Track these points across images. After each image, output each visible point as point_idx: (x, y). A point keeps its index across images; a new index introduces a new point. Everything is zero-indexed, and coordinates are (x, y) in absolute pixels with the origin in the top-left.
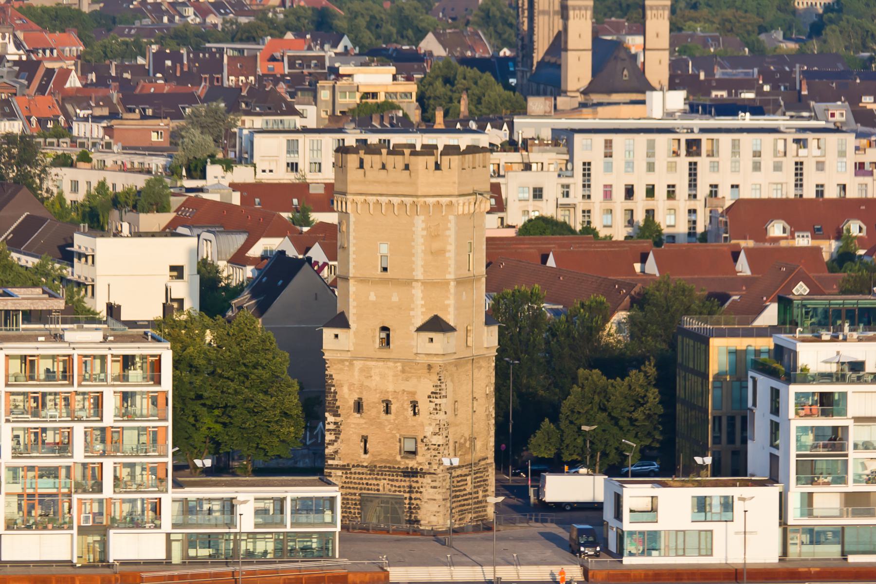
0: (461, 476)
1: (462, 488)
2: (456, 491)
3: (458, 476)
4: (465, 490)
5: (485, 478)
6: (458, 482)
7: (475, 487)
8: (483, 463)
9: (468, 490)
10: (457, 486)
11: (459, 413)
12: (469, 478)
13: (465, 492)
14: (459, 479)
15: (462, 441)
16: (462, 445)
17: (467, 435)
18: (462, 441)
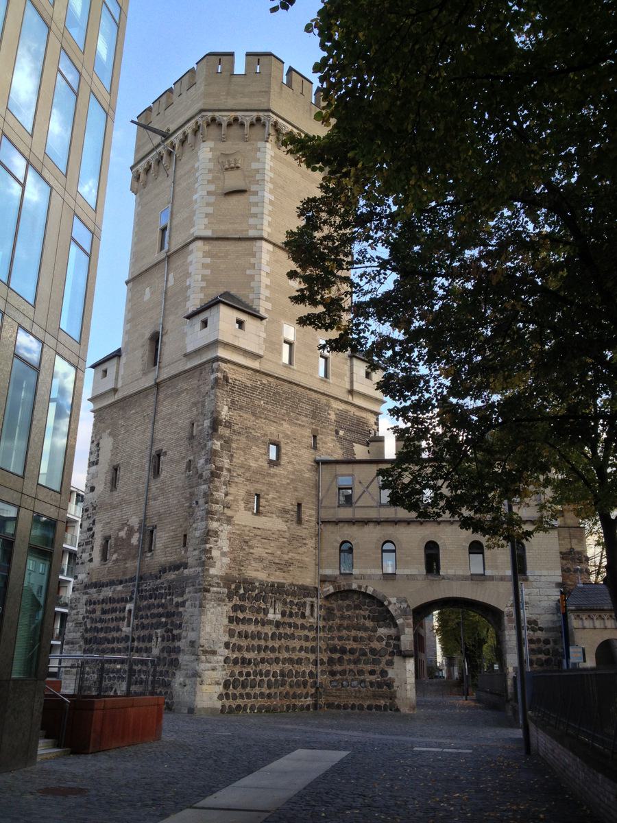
0: (112, 600)
1: (112, 625)
2: (98, 630)
3: (103, 601)
4: (118, 629)
5: (171, 609)
6: (104, 612)
7: (143, 627)
8: (172, 576)
9: (126, 630)
10: (101, 621)
11: (120, 484)
12: (130, 606)
13: (115, 634)
14: (107, 606)
15: (122, 534)
16: (123, 543)
17: (135, 521)
18: (122, 534)
